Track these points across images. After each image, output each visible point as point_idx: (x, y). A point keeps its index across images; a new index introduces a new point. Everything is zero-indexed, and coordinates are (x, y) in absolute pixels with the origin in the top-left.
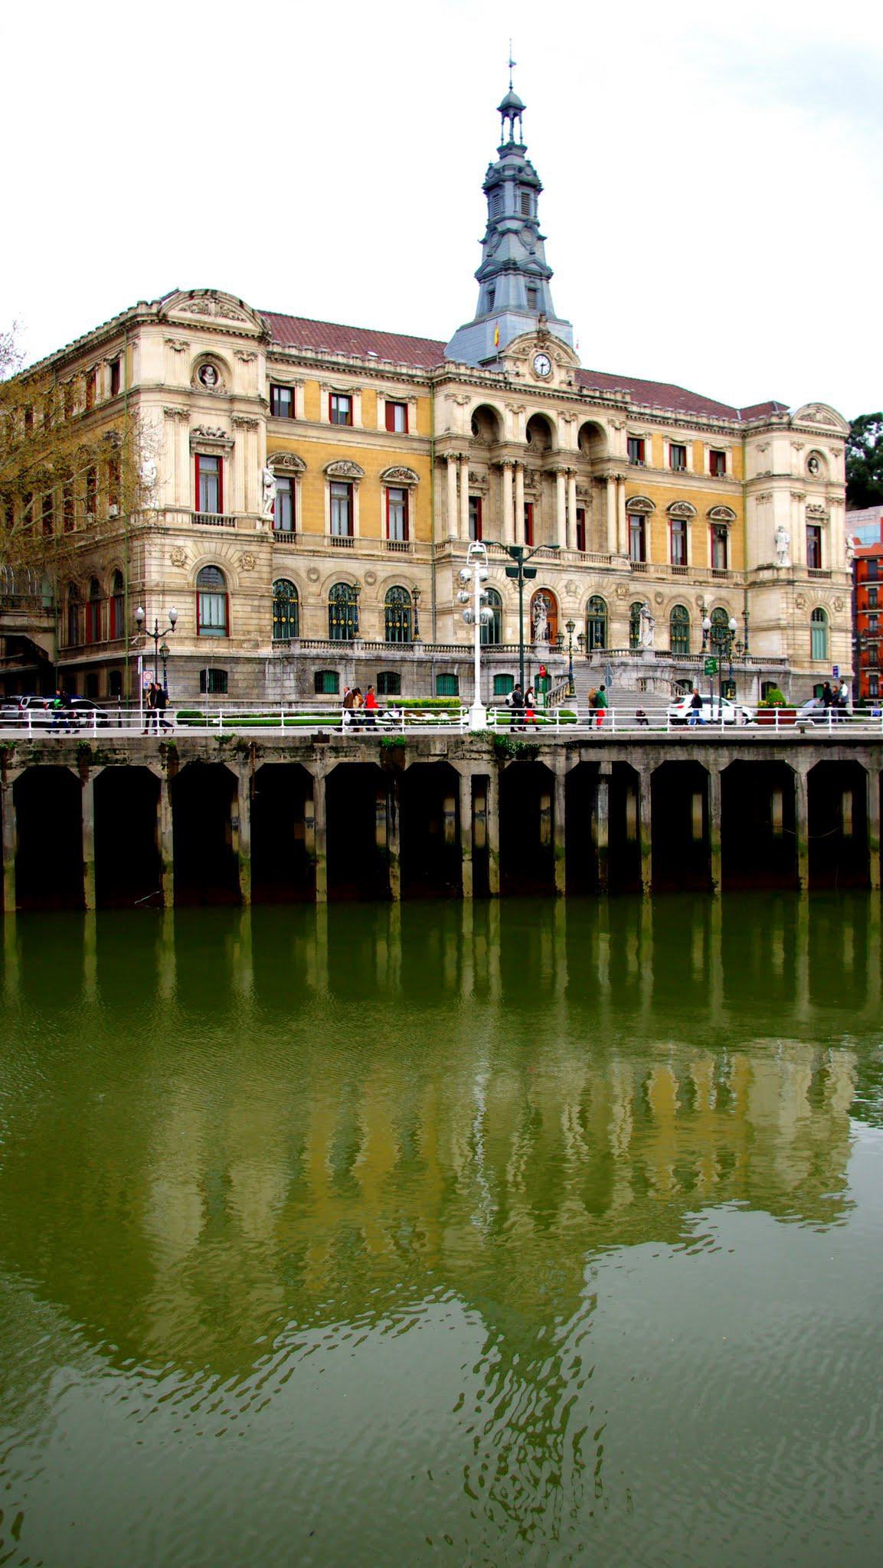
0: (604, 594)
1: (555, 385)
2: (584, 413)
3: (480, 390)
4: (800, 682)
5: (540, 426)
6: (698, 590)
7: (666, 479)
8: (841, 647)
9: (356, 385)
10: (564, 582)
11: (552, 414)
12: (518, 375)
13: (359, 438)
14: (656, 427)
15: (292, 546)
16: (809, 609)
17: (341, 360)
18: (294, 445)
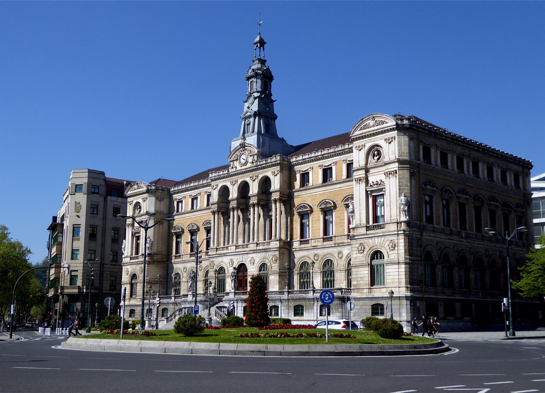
0: (267, 262)
1: (249, 165)
2: (261, 173)
3: (221, 180)
4: (361, 302)
5: (244, 188)
6: (339, 249)
7: (321, 189)
8: (396, 278)
9: (199, 192)
10: (249, 259)
11: (248, 180)
12: (232, 168)
13: (199, 213)
14: (315, 163)
15: (180, 260)
16: (368, 253)
17: (192, 185)
18: (182, 222)
